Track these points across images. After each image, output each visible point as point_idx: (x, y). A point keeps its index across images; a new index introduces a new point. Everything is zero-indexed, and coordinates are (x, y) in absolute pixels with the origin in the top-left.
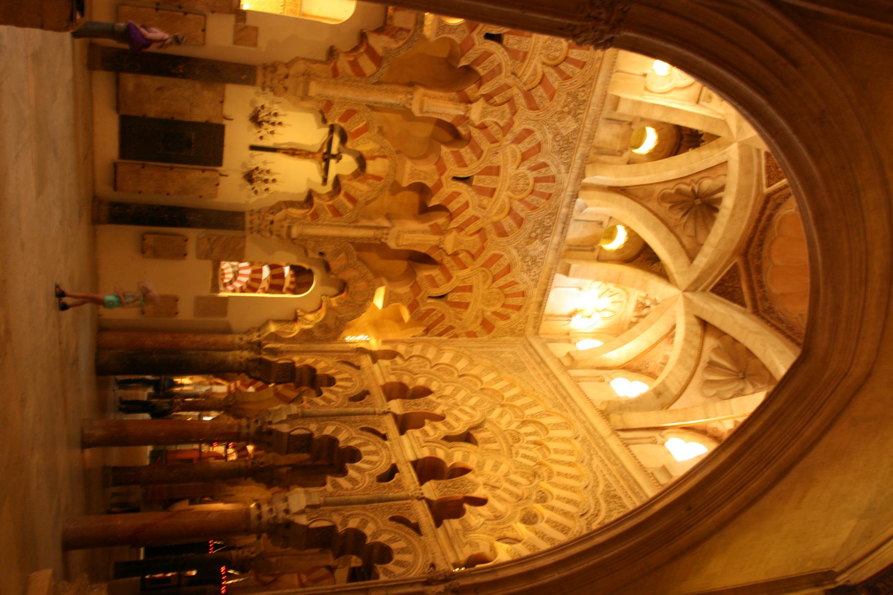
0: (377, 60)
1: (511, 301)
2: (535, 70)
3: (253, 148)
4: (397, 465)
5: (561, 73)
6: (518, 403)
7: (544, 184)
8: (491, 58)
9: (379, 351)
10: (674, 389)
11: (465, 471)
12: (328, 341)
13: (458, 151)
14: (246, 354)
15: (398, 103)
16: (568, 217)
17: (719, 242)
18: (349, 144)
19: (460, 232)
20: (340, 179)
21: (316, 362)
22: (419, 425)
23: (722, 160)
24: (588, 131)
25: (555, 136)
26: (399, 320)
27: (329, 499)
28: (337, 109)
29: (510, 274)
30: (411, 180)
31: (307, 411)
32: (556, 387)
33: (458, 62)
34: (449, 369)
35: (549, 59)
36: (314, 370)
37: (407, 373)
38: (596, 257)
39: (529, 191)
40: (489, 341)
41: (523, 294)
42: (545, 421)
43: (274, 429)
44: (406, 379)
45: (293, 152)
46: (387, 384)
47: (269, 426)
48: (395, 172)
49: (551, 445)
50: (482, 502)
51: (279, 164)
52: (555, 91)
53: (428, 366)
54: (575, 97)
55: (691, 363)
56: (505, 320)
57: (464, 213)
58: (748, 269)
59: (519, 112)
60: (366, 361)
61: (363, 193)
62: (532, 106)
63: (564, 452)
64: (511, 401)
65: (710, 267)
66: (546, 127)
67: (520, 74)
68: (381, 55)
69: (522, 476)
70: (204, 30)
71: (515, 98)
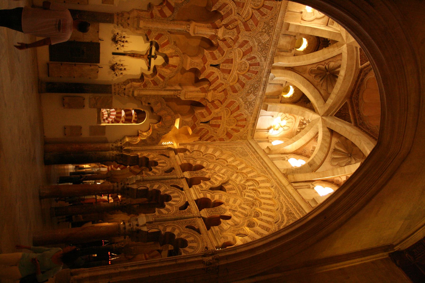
0: (172, 9)
1: (240, 123)
2: (248, 12)
3: (114, 54)
4: (189, 202)
5: (261, 13)
6: (244, 171)
7: (254, 67)
8: (227, 6)
9: (178, 149)
10: (318, 162)
11: (221, 203)
13: (213, 52)
14: (115, 152)
15: (183, 29)
16: (266, 82)
17: (338, 92)
18: (160, 51)
20: (157, 67)
21: (149, 155)
22: (198, 183)
23: (339, 53)
24: (275, 40)
25: (258, 44)
26: (187, 134)
27: (157, 219)
28: (154, 34)
29: (239, 110)
30: (191, 67)
31: (145, 178)
32: (262, 163)
33: (211, 9)
34: (211, 156)
35: (255, 6)
36: (148, 159)
37: (192, 159)
38: (280, 101)
39: (247, 70)
40: (230, 142)
41: (246, 120)
42: (258, 179)
43: (130, 187)
44: (191, 162)
45: (133, 55)
46: (182, 164)
47: (127, 186)
48: (183, 63)
49: (260, 190)
50: (229, 218)
51: (127, 61)
52: (259, 21)
53: (202, 155)
54: (268, 24)
55: (326, 150)
56: (238, 132)
59: (241, 32)
60: (172, 154)
62: (248, 29)
63: (266, 193)
64: (241, 171)
65: (334, 104)
67: (241, 14)
68: (174, 7)
69: (247, 205)
71: (239, 26)
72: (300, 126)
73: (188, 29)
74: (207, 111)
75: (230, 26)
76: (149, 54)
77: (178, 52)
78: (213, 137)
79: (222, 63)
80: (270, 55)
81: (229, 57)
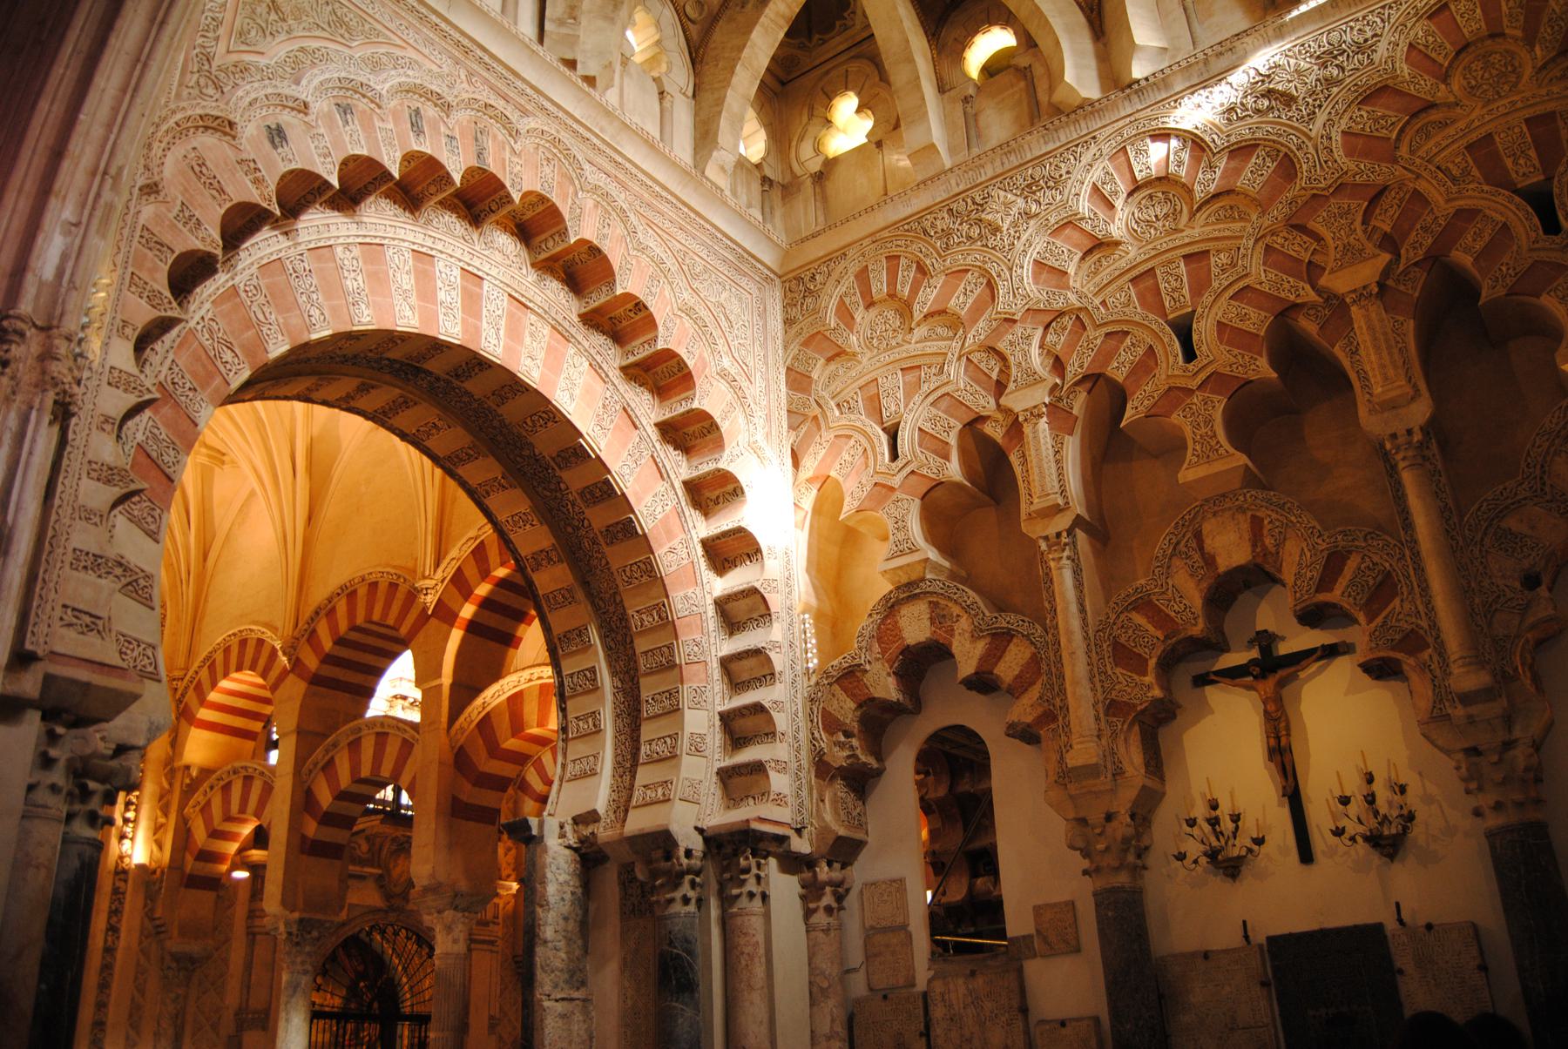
0: (1000, 640)
2: (926, 339)
8: (927, 427)
15: (1065, 561)
18: (1198, 629)
19: (1318, 266)
24: (998, 163)
29: (1390, 83)
30: (1221, 451)
33: (958, 485)
48: (1224, 496)
61: (1304, 545)
66: (1019, 246)
67: (940, 359)
68: (988, 640)
70: (1063, 1024)
71: (982, 337)
75: (997, 370)
77: (1174, 541)
80: (1064, 140)
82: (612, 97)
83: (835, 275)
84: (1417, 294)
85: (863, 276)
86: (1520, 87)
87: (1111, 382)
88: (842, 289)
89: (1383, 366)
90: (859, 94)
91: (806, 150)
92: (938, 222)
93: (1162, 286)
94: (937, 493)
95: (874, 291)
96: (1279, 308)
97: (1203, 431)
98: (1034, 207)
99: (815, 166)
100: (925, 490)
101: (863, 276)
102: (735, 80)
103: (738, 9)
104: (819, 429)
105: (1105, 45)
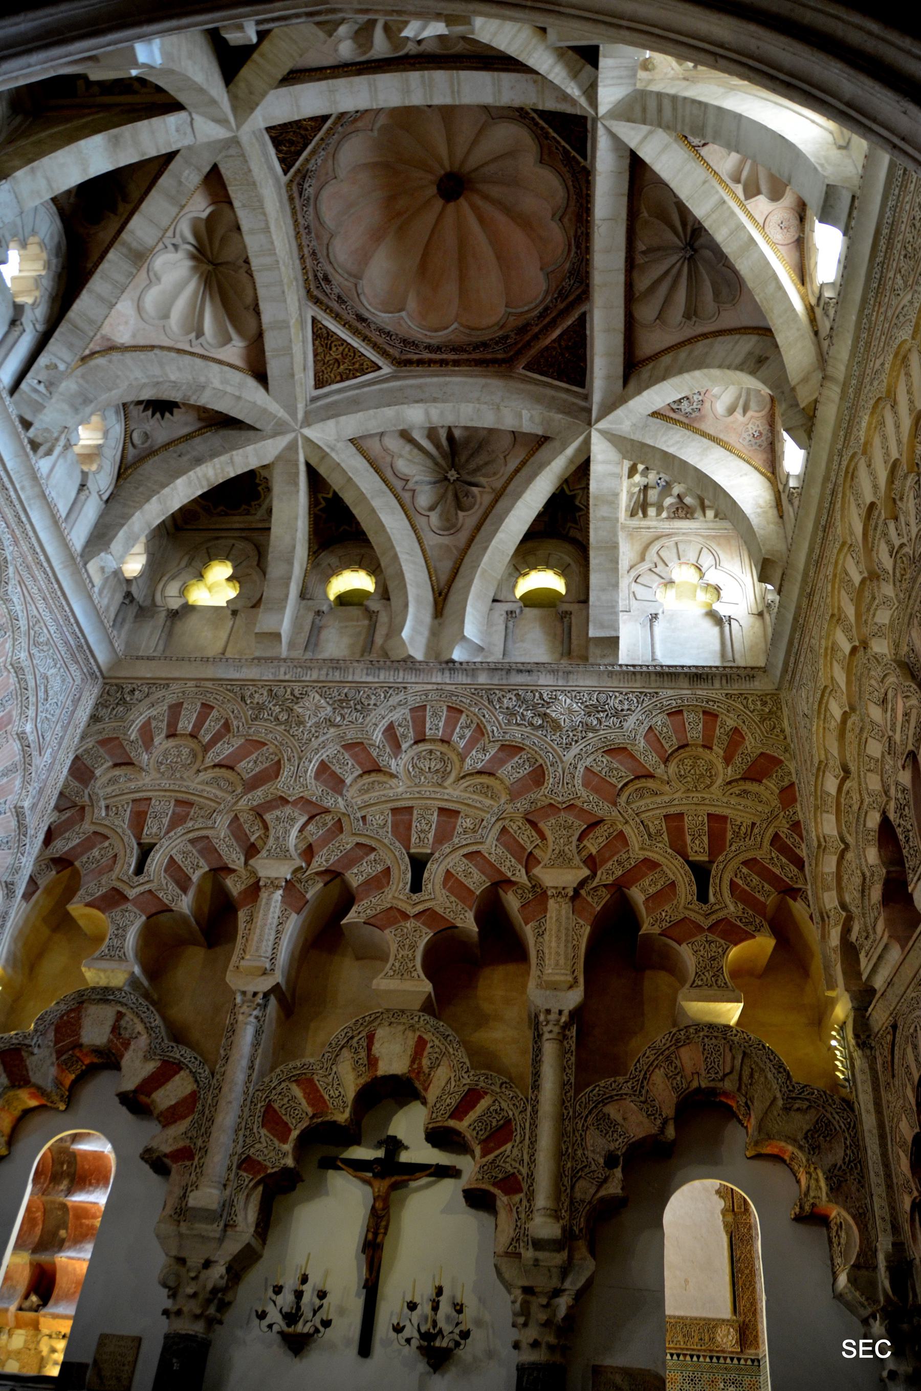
7: (428, 725)
8: (178, 858)
12: (854, 1126)
15: (252, 1019)
16: (494, 669)
18: (343, 1117)
19: (535, 858)
24: (324, 672)
29: (629, 747)
30: (414, 974)
33: (183, 918)
39: (444, 748)
44: (876, 894)
48: (403, 1011)
54: (260, 707)
55: (700, 348)
57: (492, 859)
58: (528, 345)
59: (280, 793)
61: (453, 1075)
66: (315, 743)
68: (158, 1064)
71: (255, 803)
72: (692, 514)
73: (249, 996)
74: (634, 881)
76: (370, 1175)
77: (350, 1034)
78: (776, 836)
79: (407, 848)
80: (382, 678)
81: (381, 822)
82: (43, 465)
83: (153, 698)
84: (598, 909)
85: (175, 709)
86: (713, 789)
87: (346, 886)
88: (153, 712)
89: (558, 954)
90: (235, 567)
91: (172, 589)
92: (257, 696)
93: (414, 825)
94: (163, 918)
95: (180, 725)
96: (498, 878)
97: (406, 952)
98: (338, 719)
99: (175, 604)
100: (154, 910)
101: (175, 709)
102: (147, 507)
103: (175, 455)
104: (82, 820)
105: (440, 624)
